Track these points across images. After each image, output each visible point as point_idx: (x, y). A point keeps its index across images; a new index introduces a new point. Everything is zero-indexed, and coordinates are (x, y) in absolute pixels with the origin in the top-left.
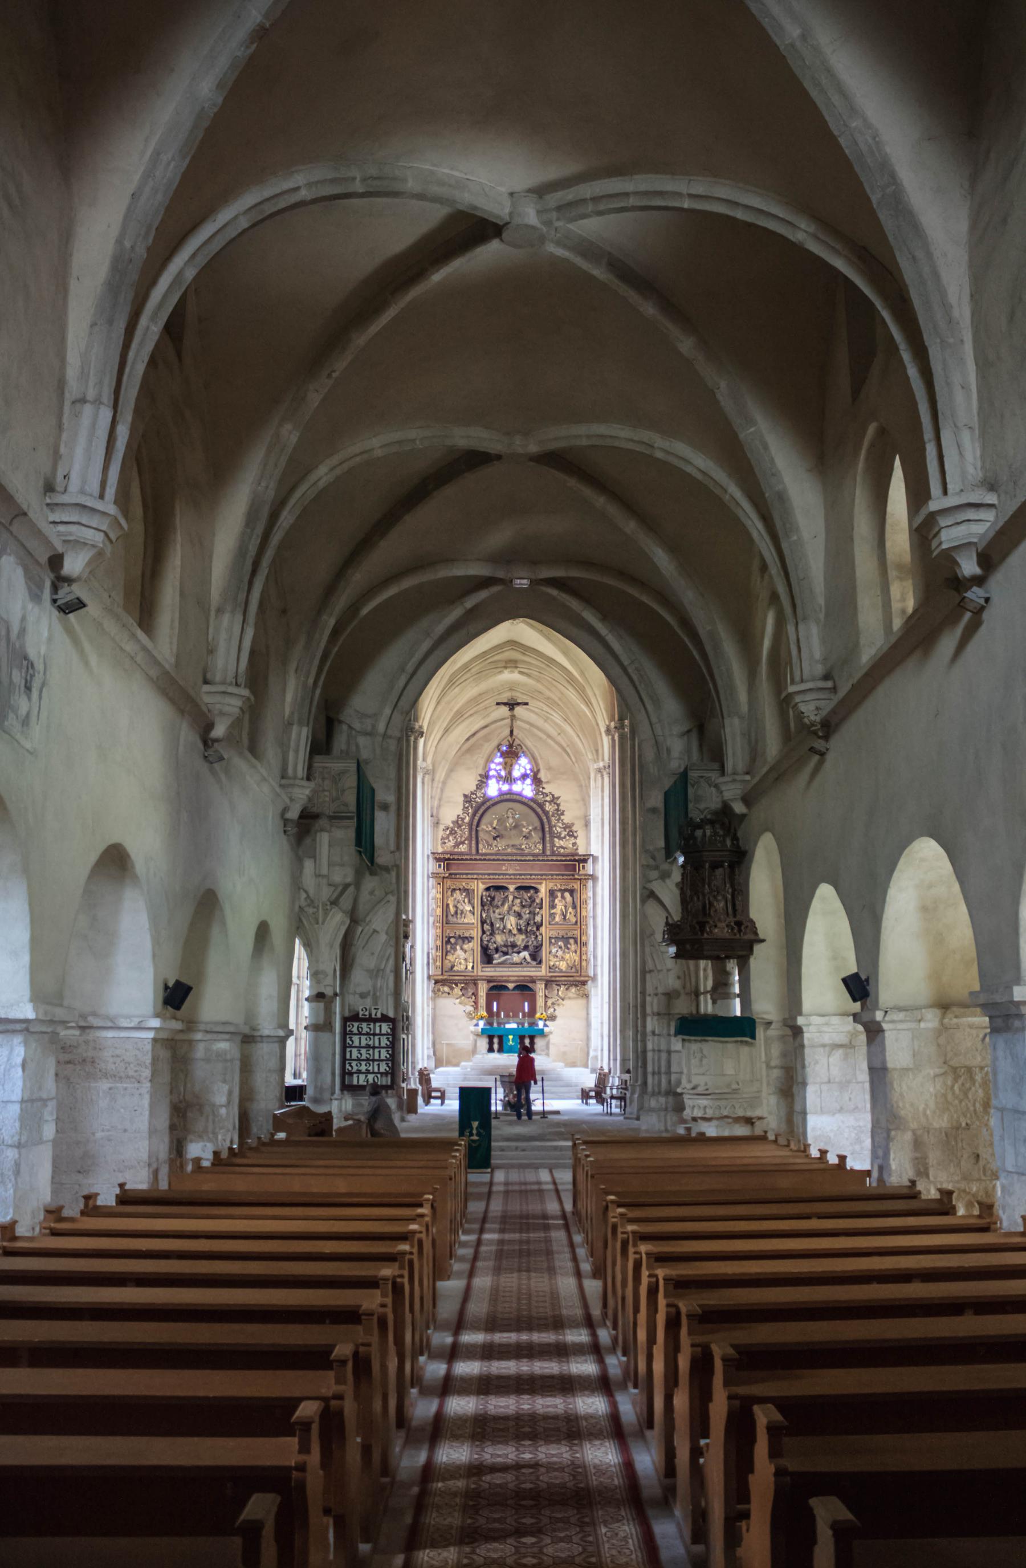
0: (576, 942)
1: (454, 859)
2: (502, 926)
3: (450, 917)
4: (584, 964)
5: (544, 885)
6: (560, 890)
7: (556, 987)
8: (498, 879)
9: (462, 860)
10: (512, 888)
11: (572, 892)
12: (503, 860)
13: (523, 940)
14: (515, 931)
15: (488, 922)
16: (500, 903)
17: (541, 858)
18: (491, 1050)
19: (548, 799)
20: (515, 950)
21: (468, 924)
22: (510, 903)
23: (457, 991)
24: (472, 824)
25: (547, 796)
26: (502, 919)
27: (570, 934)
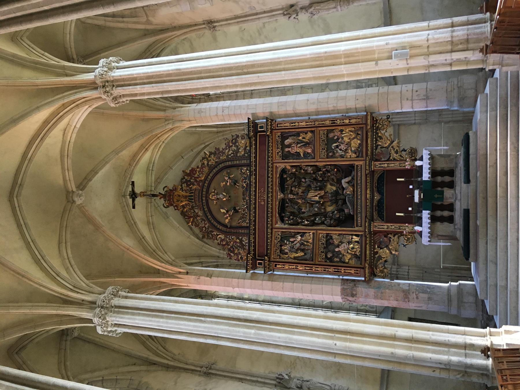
0: (332, 131)
1: (254, 250)
2: (317, 205)
3: (308, 256)
4: (353, 121)
6: (282, 149)
7: (379, 150)
8: (272, 209)
10: (281, 196)
11: (284, 137)
13: (331, 185)
14: (322, 192)
17: (253, 168)
19: (206, 162)
20: (340, 192)
21: (313, 240)
22: (295, 197)
24: (226, 232)
26: (312, 205)
27: (324, 138)
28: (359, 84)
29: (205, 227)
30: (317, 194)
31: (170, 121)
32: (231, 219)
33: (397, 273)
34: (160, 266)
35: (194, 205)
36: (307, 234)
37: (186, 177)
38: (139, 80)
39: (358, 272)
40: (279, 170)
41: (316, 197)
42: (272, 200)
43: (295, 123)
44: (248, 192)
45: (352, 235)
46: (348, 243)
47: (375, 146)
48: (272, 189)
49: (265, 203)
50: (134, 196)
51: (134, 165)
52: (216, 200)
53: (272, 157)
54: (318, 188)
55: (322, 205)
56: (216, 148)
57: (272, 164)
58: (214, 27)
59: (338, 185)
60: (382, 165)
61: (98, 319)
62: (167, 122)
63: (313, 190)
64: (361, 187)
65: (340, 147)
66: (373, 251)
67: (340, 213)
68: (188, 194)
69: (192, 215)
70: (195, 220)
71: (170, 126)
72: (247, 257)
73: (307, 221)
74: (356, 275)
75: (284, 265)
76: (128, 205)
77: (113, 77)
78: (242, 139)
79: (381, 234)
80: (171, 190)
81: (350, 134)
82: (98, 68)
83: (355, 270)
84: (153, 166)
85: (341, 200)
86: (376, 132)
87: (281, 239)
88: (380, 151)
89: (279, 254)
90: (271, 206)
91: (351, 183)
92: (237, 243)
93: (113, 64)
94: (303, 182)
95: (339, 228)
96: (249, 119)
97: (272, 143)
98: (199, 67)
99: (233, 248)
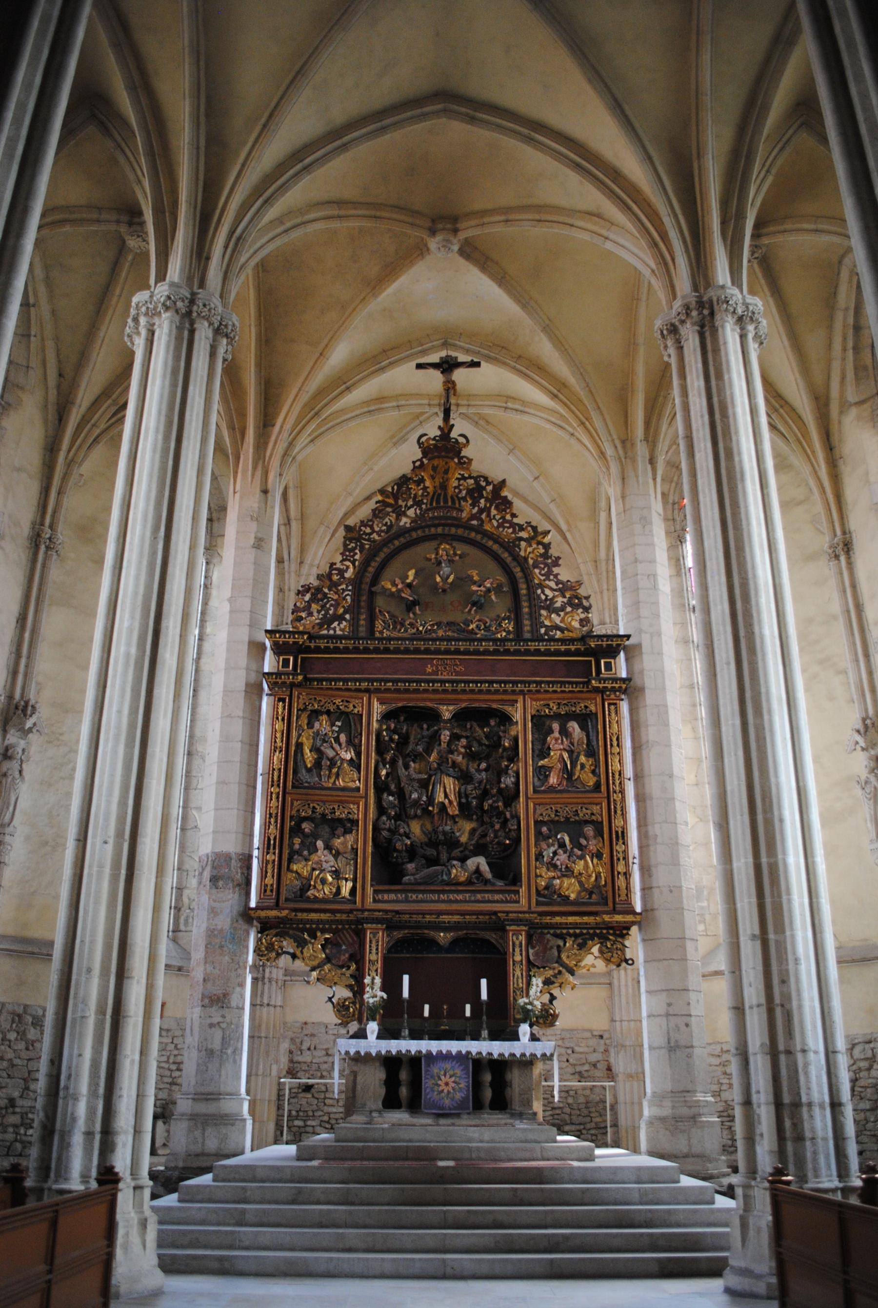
0: (599, 833)
1: (318, 650)
2: (424, 798)
3: (303, 774)
4: (621, 882)
5: (519, 705)
6: (557, 716)
8: (416, 691)
9: (337, 650)
10: (447, 711)
11: (585, 719)
12: (427, 651)
13: (473, 832)
14: (453, 810)
15: (393, 787)
16: (420, 748)
18: (391, 1102)
19: (524, 534)
20: (456, 852)
21: (344, 789)
22: (444, 745)
23: (315, 950)
24: (361, 583)
25: (522, 528)
26: (424, 785)
28: (705, 893)
29: (370, 534)
30: (452, 797)
31: (621, 452)
32: (392, 595)
33: (266, 980)
34: (282, 427)
35: (424, 506)
36: (356, 775)
37: (490, 488)
38: (717, 385)
39: (268, 892)
40: (509, 709)
41: (442, 795)
42: (436, 691)
43: (618, 745)
44: (456, 635)
45: (355, 880)
46: (336, 871)
47: (562, 934)
48: (464, 691)
49: (429, 674)
50: (446, 366)
51: (518, 367)
52: (436, 558)
53: (538, 692)
54: (463, 800)
55: (426, 811)
56: (559, 558)
57: (522, 692)
58: (837, 557)
59: (472, 848)
60: (517, 950)
61: (166, 293)
62: (618, 443)
63: (460, 789)
64: (466, 901)
65: (560, 851)
66: (317, 929)
67: (407, 851)
68: (450, 491)
69: (400, 502)
70: (389, 509)
71: (609, 451)
72: (302, 633)
73: (388, 775)
74: (263, 889)
75: (283, 719)
76: (424, 352)
77: (723, 327)
78: (581, 620)
79: (357, 946)
80: (460, 451)
81: (590, 876)
82: (741, 291)
83: (272, 885)
84: (516, 410)
85: (435, 854)
86: (595, 934)
87: (343, 713)
88: (551, 944)
89: (310, 708)
90: (421, 688)
91: (478, 879)
92: (336, 609)
93: (751, 328)
94: (479, 766)
95: (370, 849)
96: (628, 637)
97: (570, 692)
98: (749, 524)
99: (322, 600)
